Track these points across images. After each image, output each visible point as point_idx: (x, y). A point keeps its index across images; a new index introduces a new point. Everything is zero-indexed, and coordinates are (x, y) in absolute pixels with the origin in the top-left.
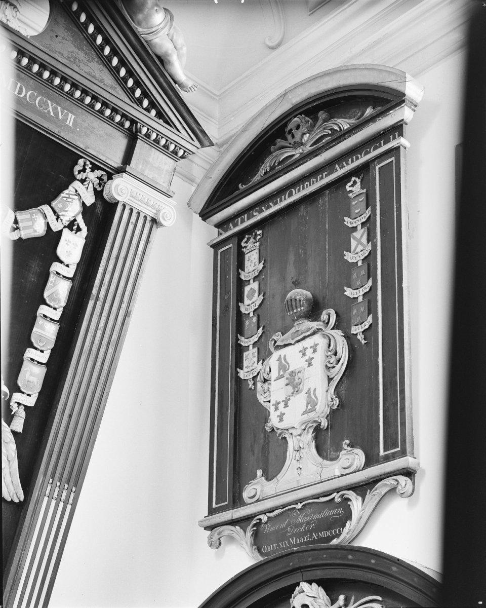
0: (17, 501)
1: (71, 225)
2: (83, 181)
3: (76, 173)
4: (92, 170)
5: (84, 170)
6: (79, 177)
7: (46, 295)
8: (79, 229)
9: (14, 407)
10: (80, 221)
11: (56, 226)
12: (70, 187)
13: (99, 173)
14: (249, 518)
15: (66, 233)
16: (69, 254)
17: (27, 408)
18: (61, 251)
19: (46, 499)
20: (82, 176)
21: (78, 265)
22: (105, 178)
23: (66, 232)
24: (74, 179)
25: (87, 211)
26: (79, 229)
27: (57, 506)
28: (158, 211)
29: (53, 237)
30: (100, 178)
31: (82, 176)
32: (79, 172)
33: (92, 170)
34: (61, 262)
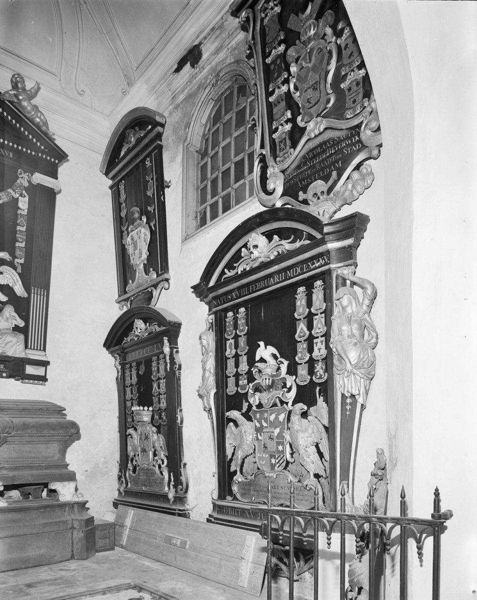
2: (22, 178)
6: (20, 176)
9: (16, 264)
10: (24, 192)
14: (128, 298)
17: (21, 264)
18: (20, 205)
19: (32, 295)
20: (21, 176)
22: (30, 175)
24: (19, 178)
25: (26, 189)
26: (25, 196)
30: (28, 176)
32: (20, 174)
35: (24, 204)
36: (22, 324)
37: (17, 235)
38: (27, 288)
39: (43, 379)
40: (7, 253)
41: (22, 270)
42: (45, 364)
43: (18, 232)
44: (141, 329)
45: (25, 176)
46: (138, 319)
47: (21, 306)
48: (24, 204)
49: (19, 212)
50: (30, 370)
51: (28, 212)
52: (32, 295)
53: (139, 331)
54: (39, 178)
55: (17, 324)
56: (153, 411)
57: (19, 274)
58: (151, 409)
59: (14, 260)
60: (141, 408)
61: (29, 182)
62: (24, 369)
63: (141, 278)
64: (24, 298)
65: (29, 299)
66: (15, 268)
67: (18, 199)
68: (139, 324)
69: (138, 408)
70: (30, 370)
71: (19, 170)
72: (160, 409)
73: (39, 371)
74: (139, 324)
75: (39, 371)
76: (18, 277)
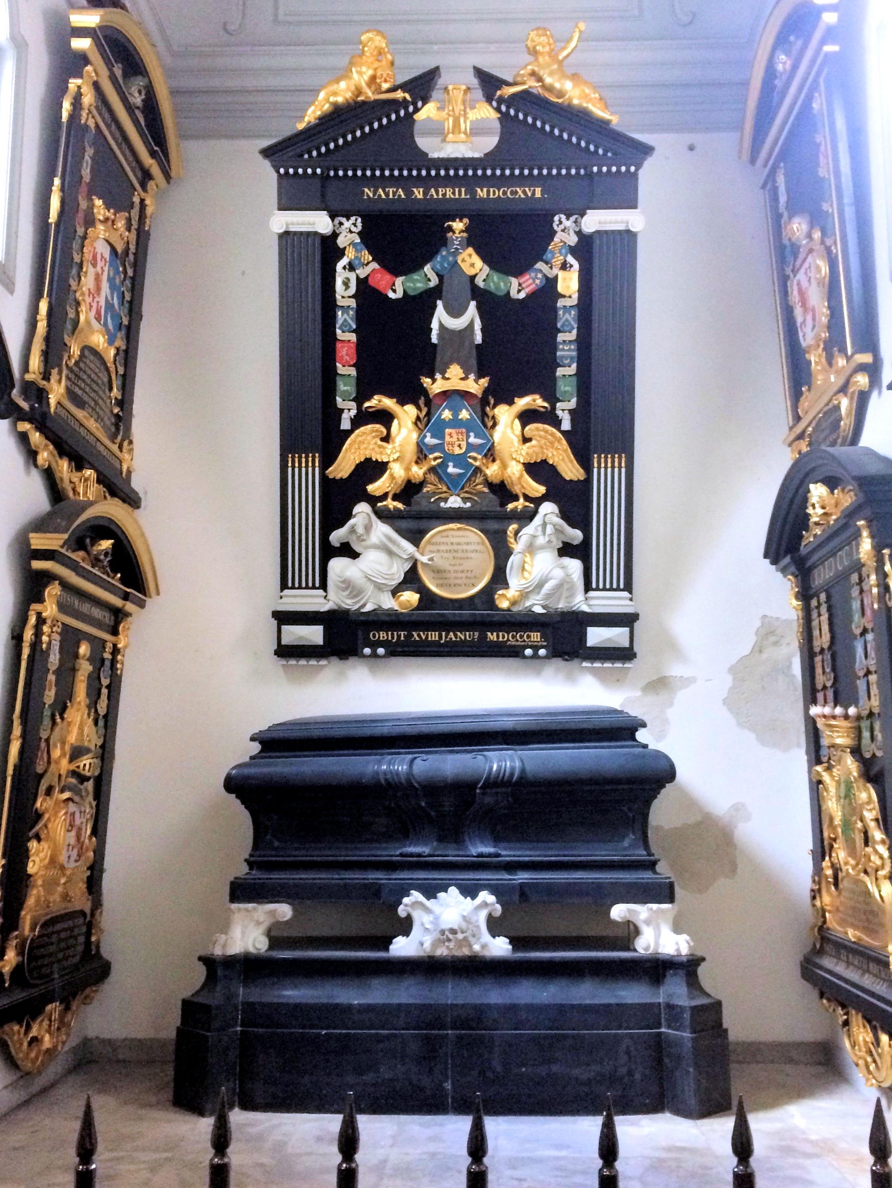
0: (582, 479)
1: (564, 266)
3: (555, 227)
4: (568, 219)
5: (561, 222)
7: (559, 325)
8: (571, 266)
9: (559, 413)
10: (570, 259)
11: (551, 274)
12: (555, 239)
13: (573, 219)
15: (561, 275)
16: (568, 287)
18: (560, 288)
20: (562, 227)
21: (578, 291)
23: (561, 275)
26: (571, 266)
27: (613, 473)
28: (627, 223)
29: (551, 283)
30: (576, 222)
31: (562, 227)
33: (568, 219)
34: (564, 296)
35: (569, 284)
36: (576, 536)
37: (558, 353)
38: (584, 460)
39: (626, 654)
40: (537, 397)
41: (573, 421)
42: (628, 620)
43: (561, 347)
44: (823, 507)
45: (568, 223)
46: (816, 482)
47: (574, 501)
48: (569, 284)
49: (560, 303)
50: (596, 636)
51: (579, 298)
52: (595, 470)
53: (820, 511)
54: (595, 221)
55: (566, 540)
56: (859, 718)
57: (564, 433)
58: (852, 711)
59: (554, 408)
60: (839, 710)
61: (579, 233)
62: (583, 637)
63: (825, 377)
64: (579, 481)
65: (587, 483)
66: (556, 422)
67: (557, 276)
68: (817, 491)
69: (827, 710)
70: (596, 636)
71: (556, 218)
72: (871, 715)
73: (615, 636)
74: (817, 491)
75: (615, 636)
76: (564, 442)
